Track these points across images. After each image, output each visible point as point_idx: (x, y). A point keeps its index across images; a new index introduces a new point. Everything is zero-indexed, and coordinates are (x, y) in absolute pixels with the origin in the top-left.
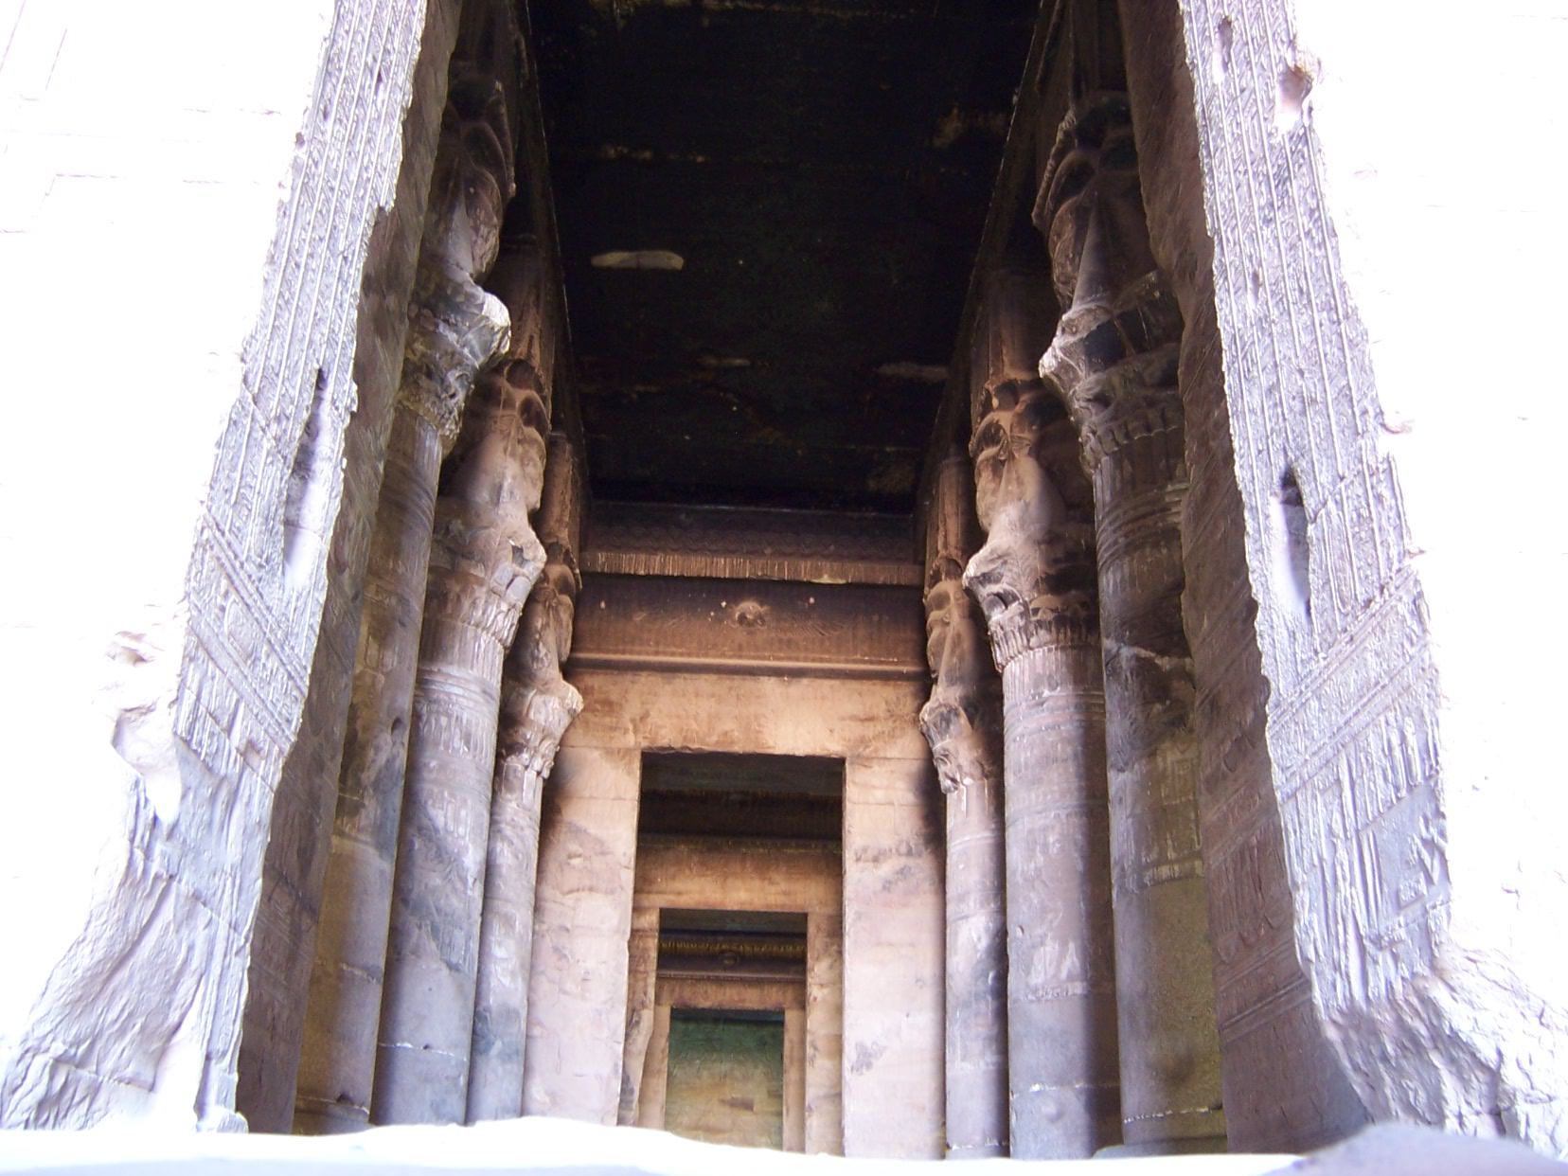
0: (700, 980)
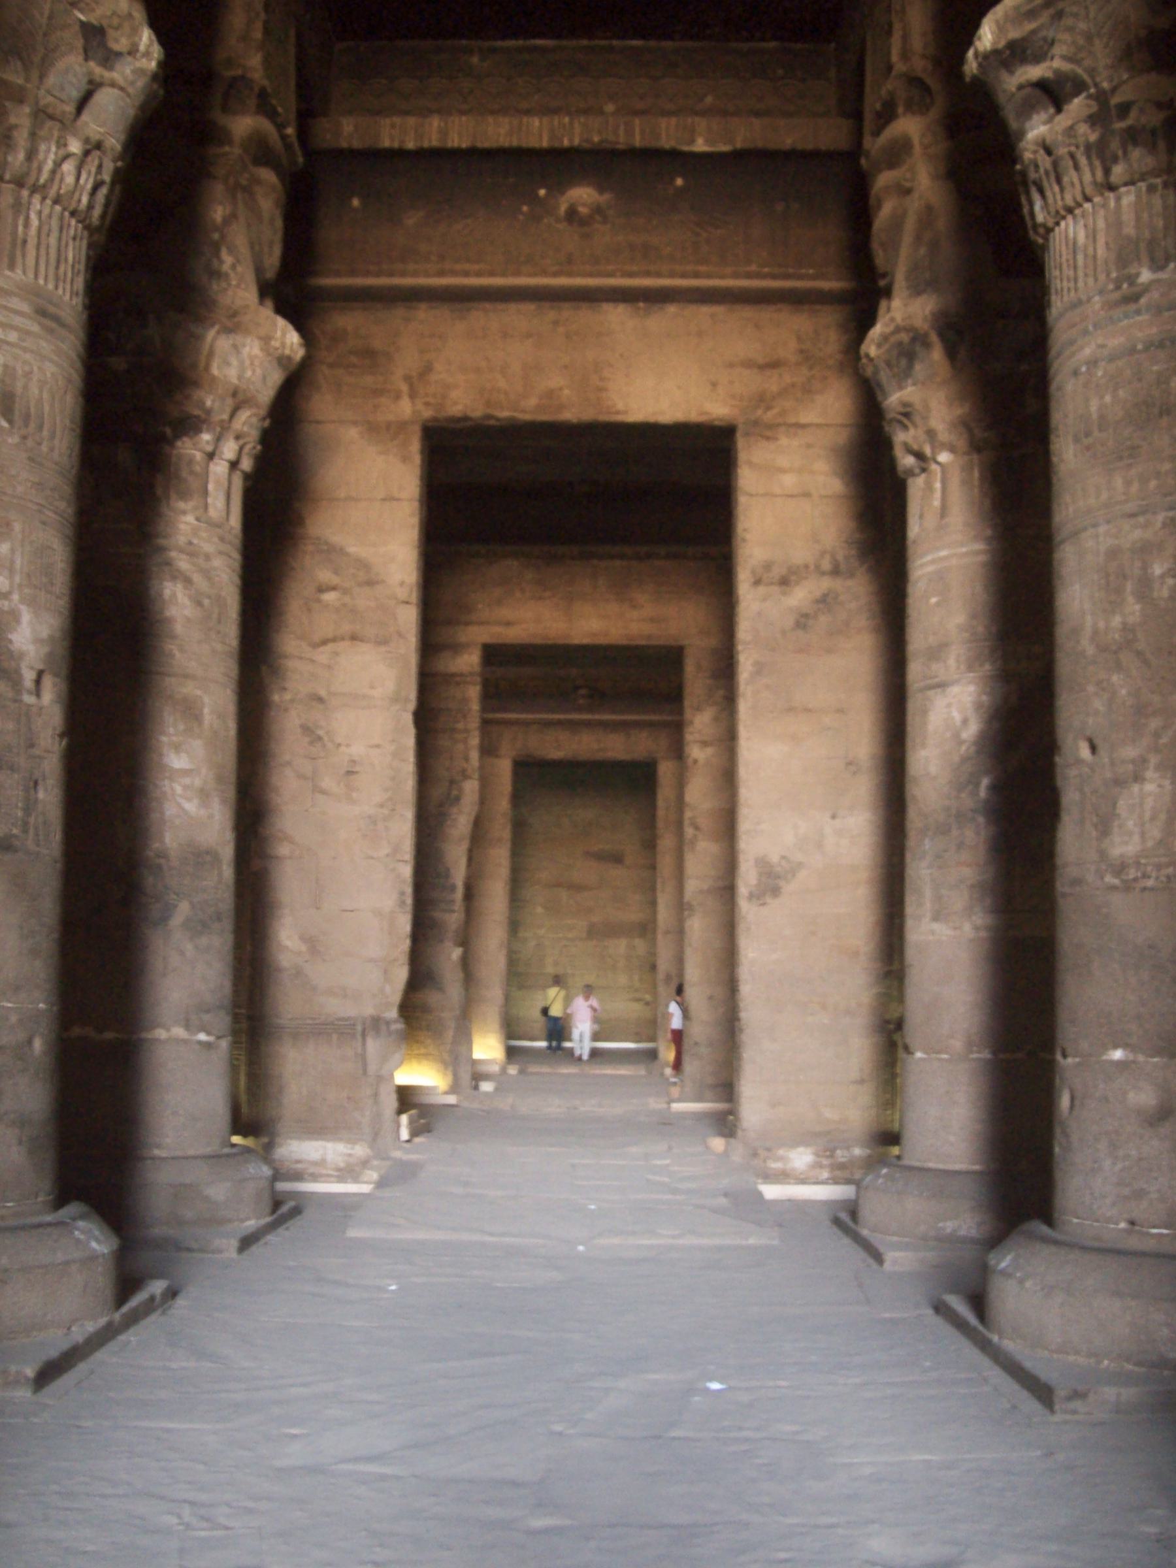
0: (548, 724)
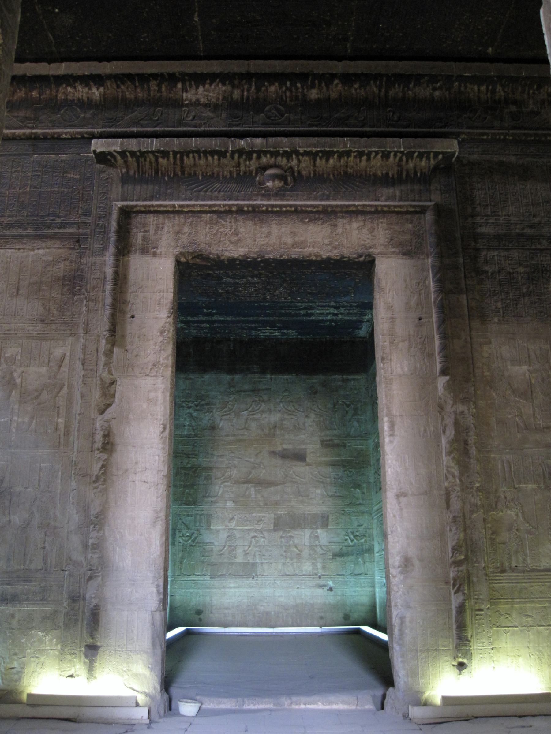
0: (229, 212)
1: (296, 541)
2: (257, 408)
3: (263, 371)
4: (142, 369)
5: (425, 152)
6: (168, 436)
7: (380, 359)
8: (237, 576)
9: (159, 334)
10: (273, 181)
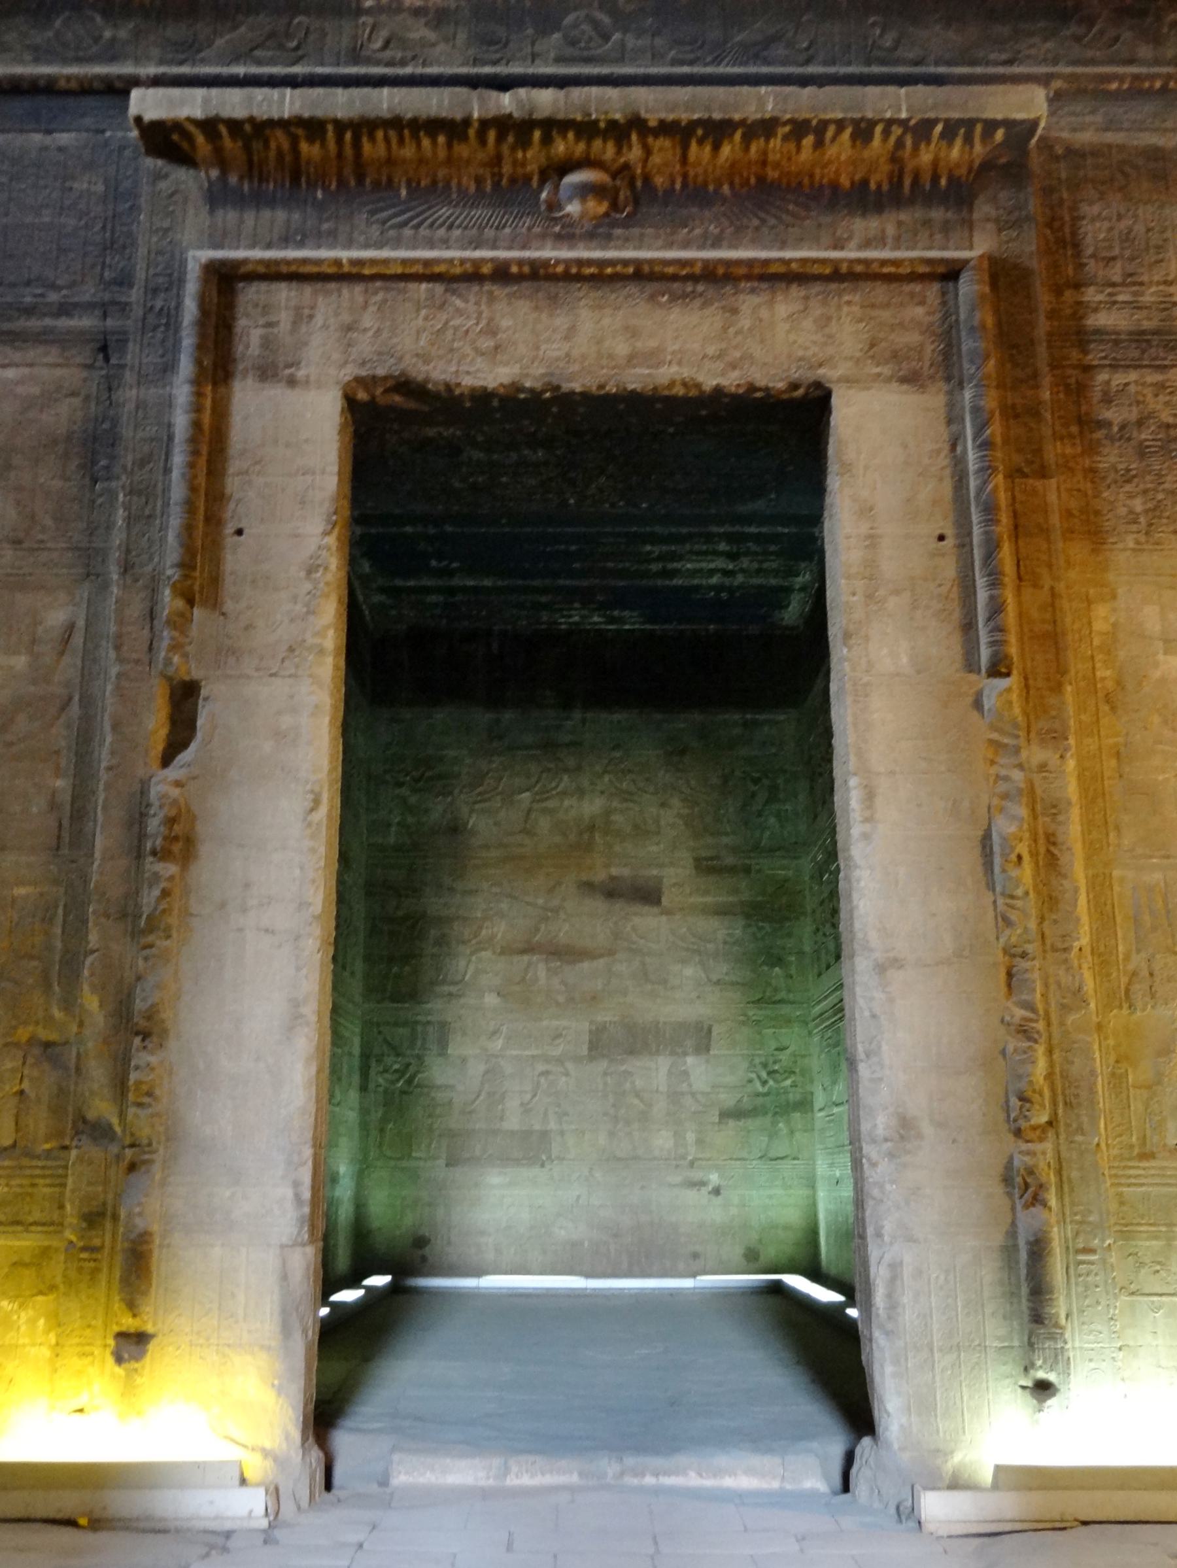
0: (473, 276)
1: (639, 1083)
2: (553, 784)
3: (566, 704)
4: (262, 659)
5: (960, 122)
6: (325, 822)
7: (840, 636)
8: (506, 1160)
9: (303, 574)
10: (583, 199)
